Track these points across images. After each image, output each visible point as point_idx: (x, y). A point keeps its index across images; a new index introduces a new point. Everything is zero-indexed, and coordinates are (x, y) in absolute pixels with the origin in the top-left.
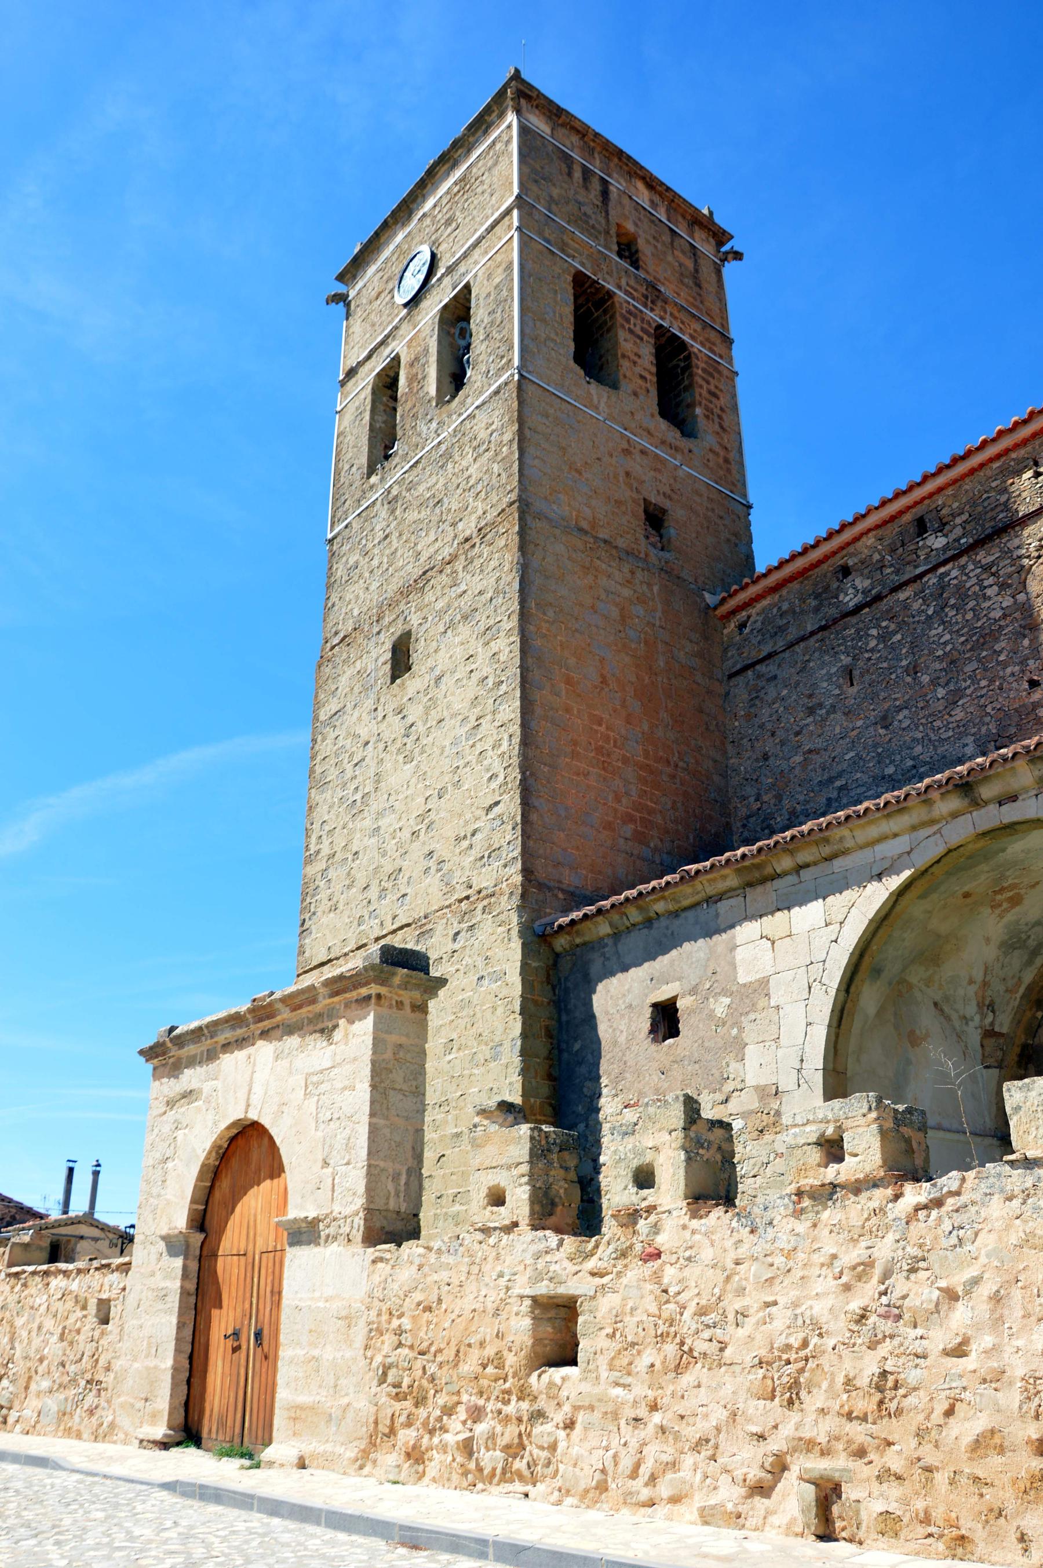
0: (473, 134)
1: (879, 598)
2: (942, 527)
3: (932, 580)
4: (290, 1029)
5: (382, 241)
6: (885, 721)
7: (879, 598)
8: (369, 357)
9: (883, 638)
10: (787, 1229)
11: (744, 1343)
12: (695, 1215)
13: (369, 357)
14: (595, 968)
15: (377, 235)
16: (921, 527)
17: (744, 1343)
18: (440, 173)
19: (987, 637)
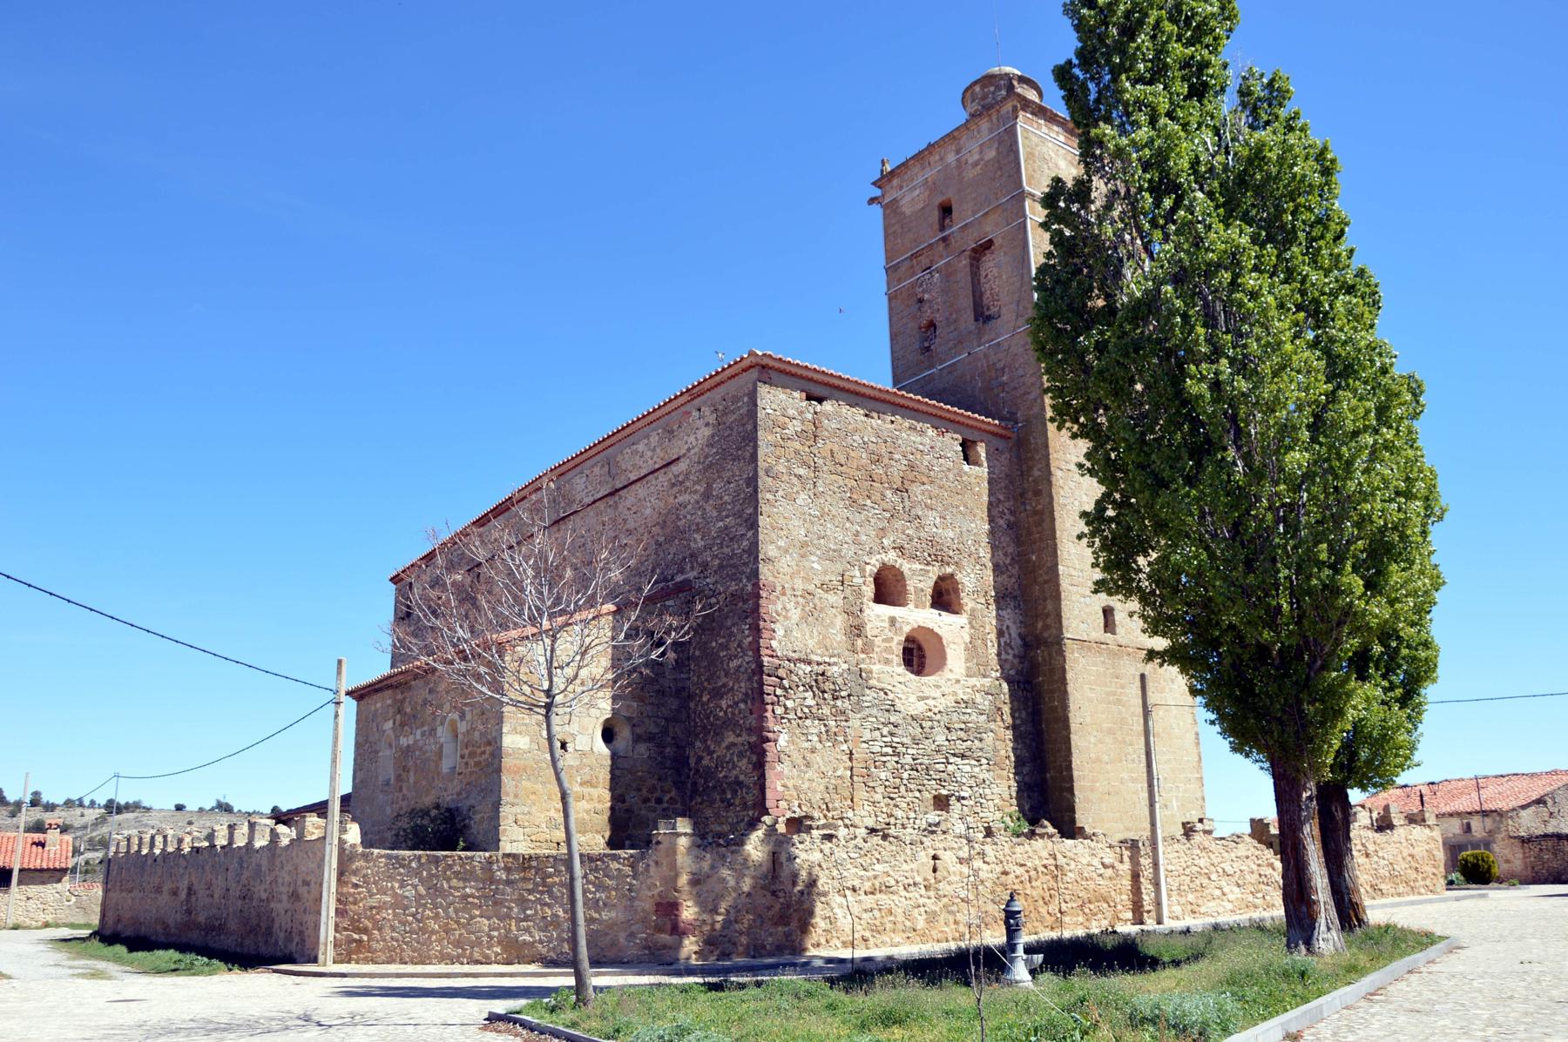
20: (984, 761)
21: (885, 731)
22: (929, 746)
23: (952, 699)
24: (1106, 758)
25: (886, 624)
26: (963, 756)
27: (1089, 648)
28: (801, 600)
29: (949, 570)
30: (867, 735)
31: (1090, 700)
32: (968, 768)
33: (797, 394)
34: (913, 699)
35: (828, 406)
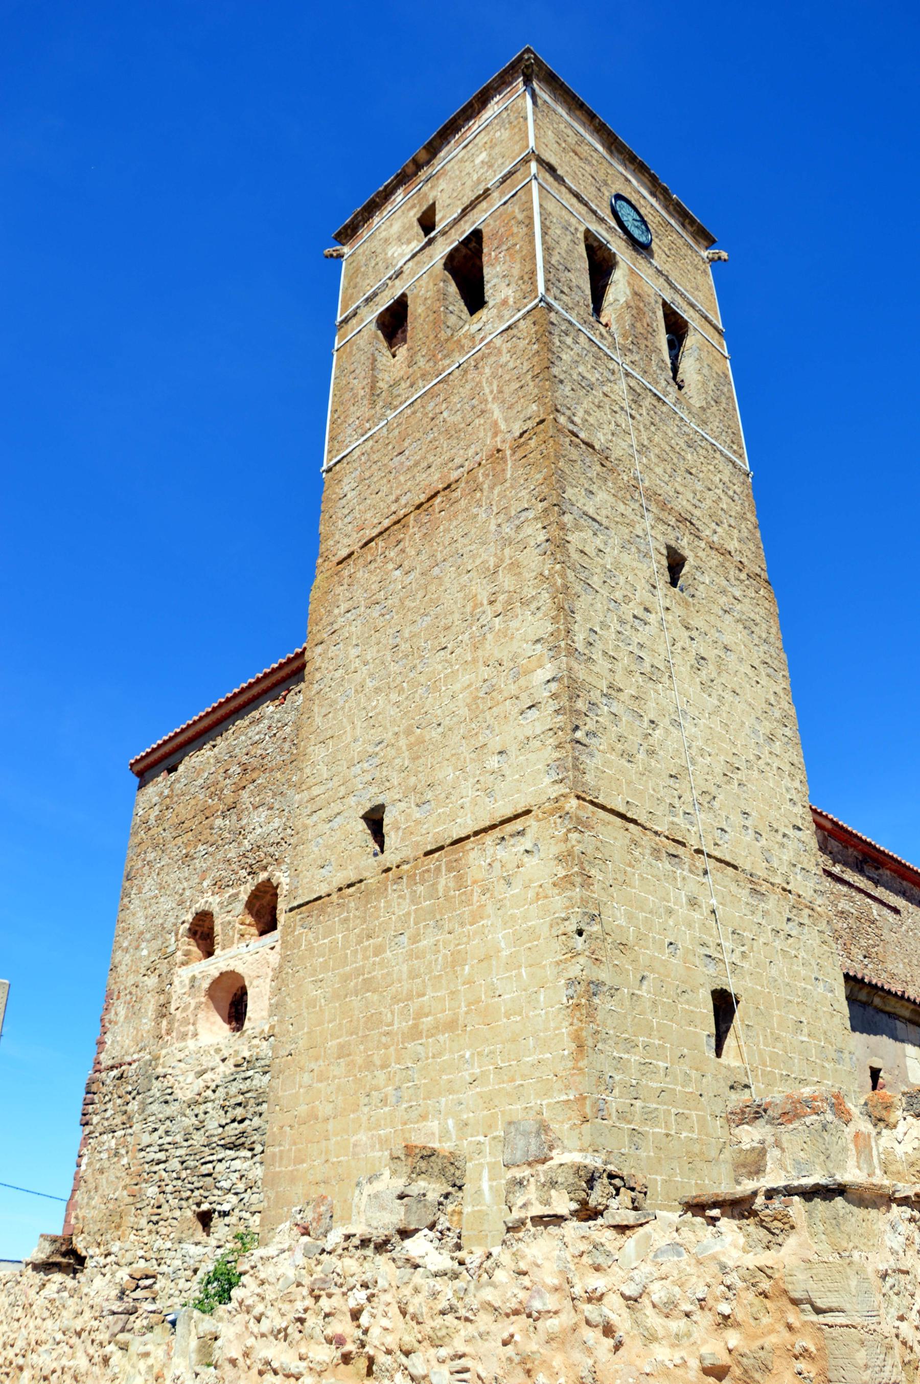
0: (675, 209)
5: (578, 113)
15: (581, 106)
18: (643, 177)
20: (258, 1148)
21: (161, 1132)
22: (198, 1139)
23: (231, 1062)
24: (324, 1109)
25: (186, 989)
26: (234, 1147)
27: (322, 911)
28: (128, 997)
29: (263, 876)
30: (146, 1139)
31: (312, 1003)
32: (237, 1164)
33: (160, 779)
34: (191, 1077)
35: (181, 768)
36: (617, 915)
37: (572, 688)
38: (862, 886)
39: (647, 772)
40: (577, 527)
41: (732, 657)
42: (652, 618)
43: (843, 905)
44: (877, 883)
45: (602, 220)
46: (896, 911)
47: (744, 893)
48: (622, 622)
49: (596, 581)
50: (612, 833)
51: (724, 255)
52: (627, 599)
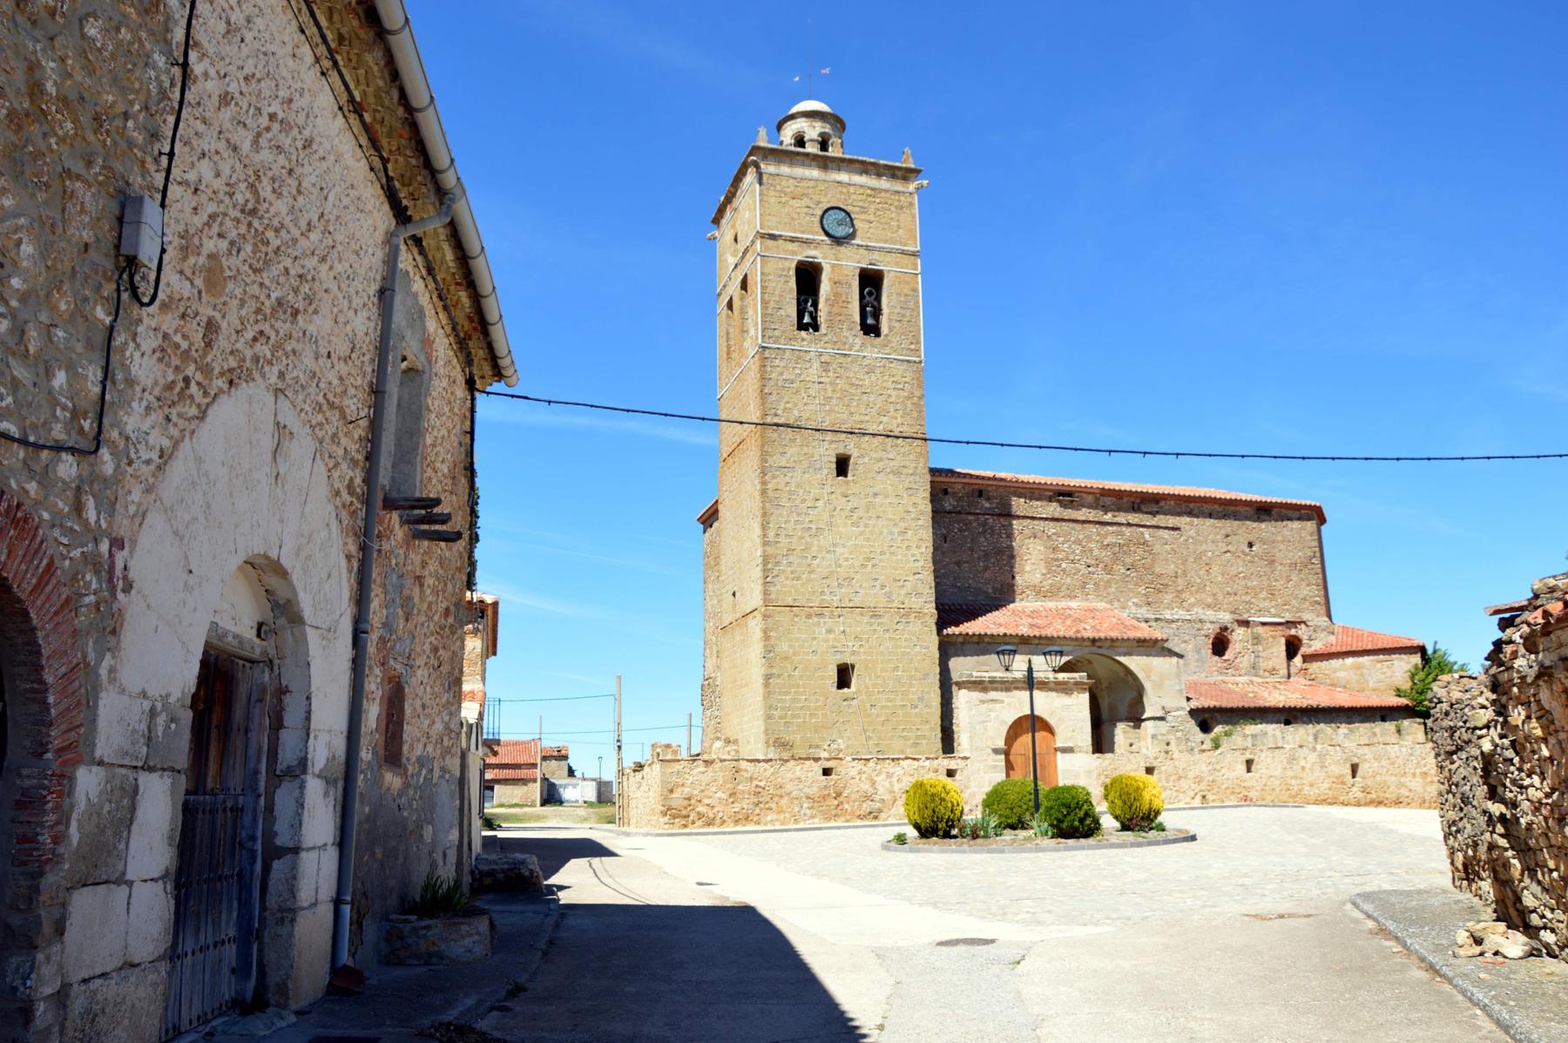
1: (959, 513)
2: (988, 499)
3: (982, 518)
4: (1052, 690)
6: (958, 564)
7: (959, 513)
8: (793, 240)
9: (960, 530)
10: (1198, 756)
11: (1191, 774)
12: (1112, 750)
13: (793, 240)
14: (951, 651)
16: (980, 494)
17: (1191, 774)
19: (1000, 552)
36: (784, 647)
37: (766, 561)
38: (1136, 521)
39: (809, 580)
40: (774, 477)
41: (878, 500)
42: (820, 504)
43: (1110, 539)
44: (1154, 514)
45: (807, 242)
46: (1174, 529)
47: (865, 619)
48: (799, 515)
49: (784, 502)
50: (783, 617)
51: (925, 182)
52: (803, 501)
